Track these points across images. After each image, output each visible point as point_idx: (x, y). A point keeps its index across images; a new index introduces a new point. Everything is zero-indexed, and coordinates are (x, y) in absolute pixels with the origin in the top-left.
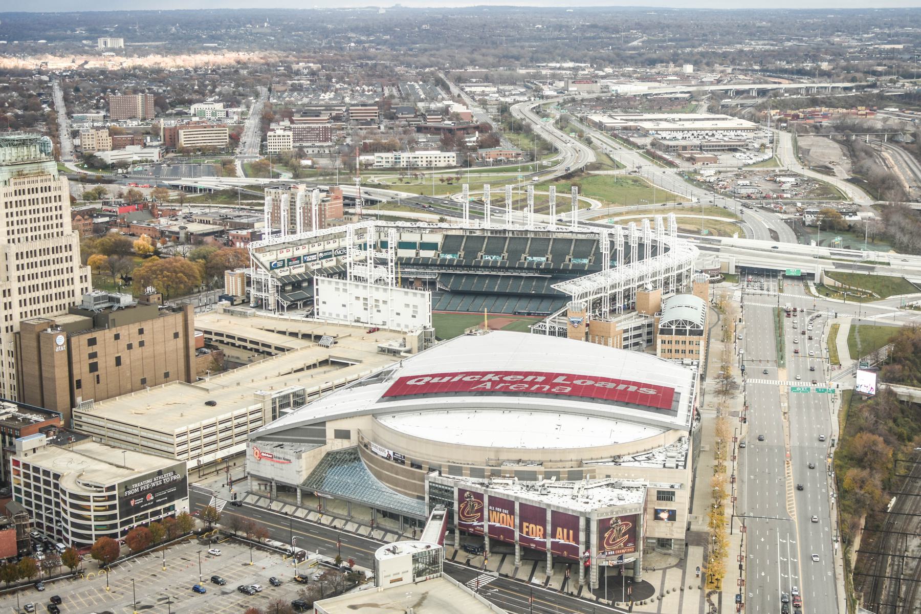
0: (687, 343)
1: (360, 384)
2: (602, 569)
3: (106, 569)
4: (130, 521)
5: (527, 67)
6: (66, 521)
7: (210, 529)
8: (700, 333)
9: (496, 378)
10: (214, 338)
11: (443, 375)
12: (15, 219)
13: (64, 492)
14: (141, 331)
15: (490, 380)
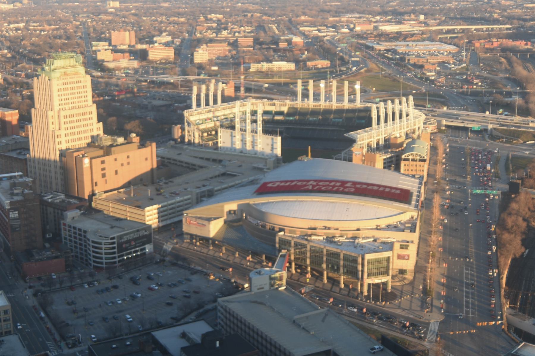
0: (418, 166)
1: (243, 186)
2: (369, 285)
3: (111, 280)
4: (123, 255)
5: (334, 17)
6: (90, 255)
7: (164, 261)
8: (424, 161)
9: (315, 183)
10: (166, 161)
11: (286, 182)
12: (63, 97)
13: (89, 240)
14: (128, 157)
15: (311, 185)
